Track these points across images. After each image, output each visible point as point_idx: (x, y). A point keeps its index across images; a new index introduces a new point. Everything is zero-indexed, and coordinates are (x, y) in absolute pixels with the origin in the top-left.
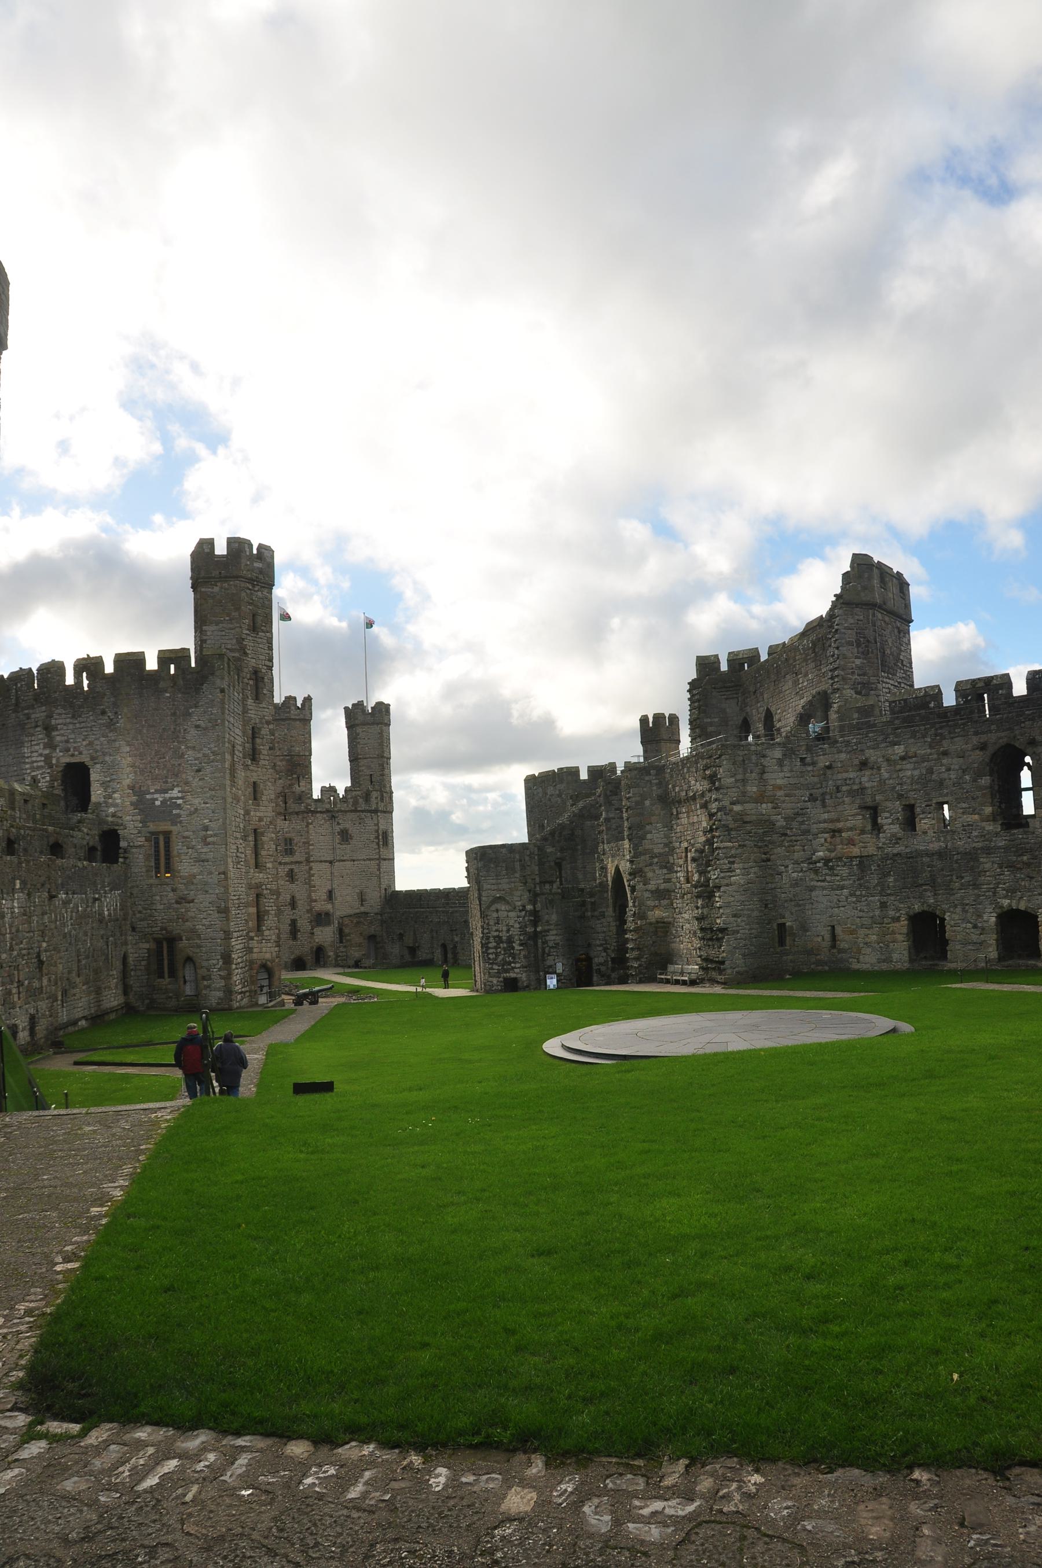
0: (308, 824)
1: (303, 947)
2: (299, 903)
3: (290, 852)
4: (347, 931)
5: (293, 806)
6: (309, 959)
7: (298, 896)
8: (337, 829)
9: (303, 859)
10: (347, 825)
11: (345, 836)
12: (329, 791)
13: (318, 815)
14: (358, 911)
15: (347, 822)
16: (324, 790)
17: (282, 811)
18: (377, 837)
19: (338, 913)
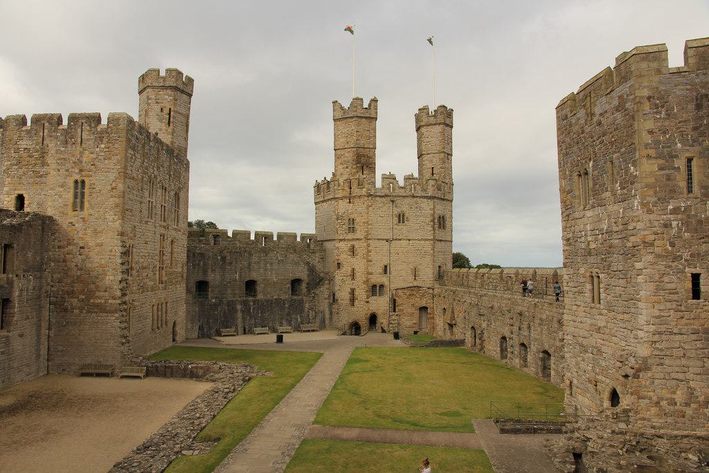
0: (368, 207)
1: (360, 312)
2: (358, 275)
3: (352, 230)
4: (399, 301)
5: (356, 191)
6: (364, 323)
7: (357, 270)
8: (396, 211)
9: (362, 237)
10: (405, 209)
11: (401, 218)
12: (390, 178)
13: (378, 199)
14: (411, 285)
15: (405, 206)
16: (384, 177)
17: (348, 195)
18: (433, 221)
19: (393, 286)
